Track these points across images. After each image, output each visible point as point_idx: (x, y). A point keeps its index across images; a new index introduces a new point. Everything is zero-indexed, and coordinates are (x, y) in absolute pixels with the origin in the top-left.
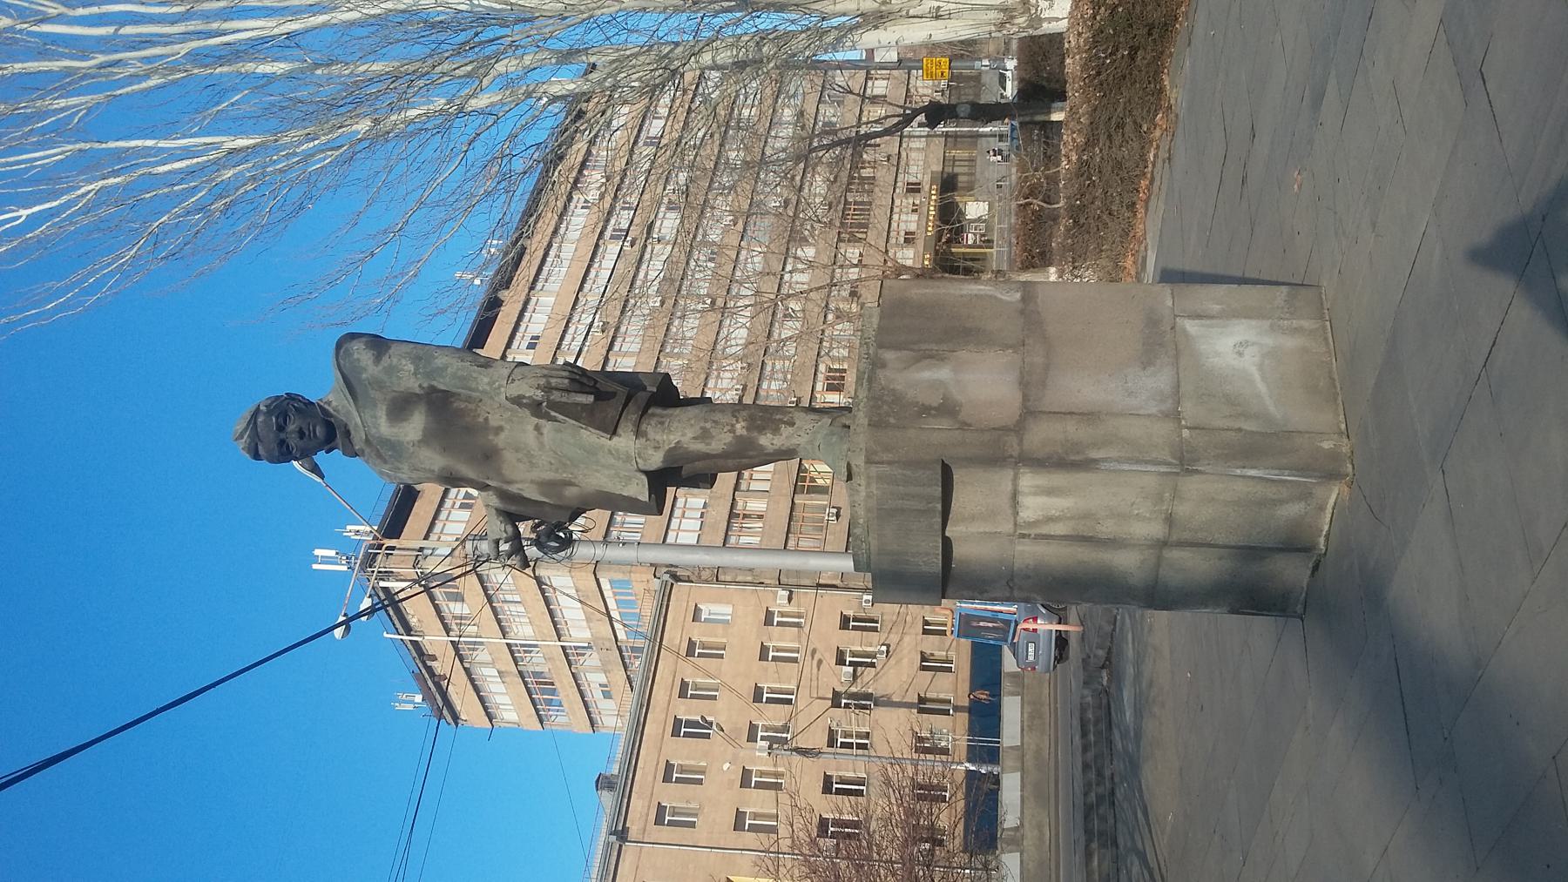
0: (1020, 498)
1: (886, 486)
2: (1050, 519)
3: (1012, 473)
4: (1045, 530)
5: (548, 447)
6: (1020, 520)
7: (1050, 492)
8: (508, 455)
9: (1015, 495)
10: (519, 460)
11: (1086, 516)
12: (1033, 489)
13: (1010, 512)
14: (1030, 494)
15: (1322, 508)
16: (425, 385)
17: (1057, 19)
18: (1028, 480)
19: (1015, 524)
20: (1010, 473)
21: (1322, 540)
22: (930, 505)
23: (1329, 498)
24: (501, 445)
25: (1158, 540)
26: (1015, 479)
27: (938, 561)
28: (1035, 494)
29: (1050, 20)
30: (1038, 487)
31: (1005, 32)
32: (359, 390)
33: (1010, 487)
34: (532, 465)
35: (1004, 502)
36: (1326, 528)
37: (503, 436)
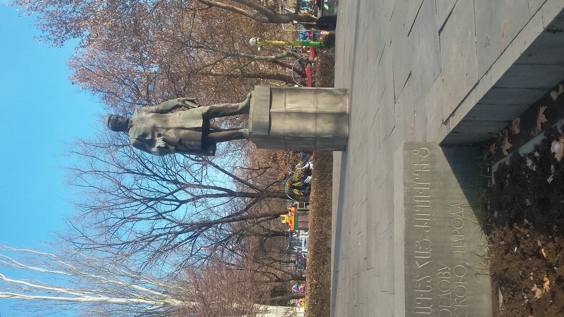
1: (258, 92)
2: (293, 108)
3: (284, 96)
4: (291, 110)
5: (181, 118)
6: (286, 109)
7: (292, 102)
8: (171, 121)
9: (285, 103)
10: (173, 122)
11: (300, 108)
12: (289, 102)
13: (284, 107)
14: (288, 103)
15: (346, 105)
16: (157, 108)
18: (288, 99)
19: (285, 109)
21: (348, 111)
22: (267, 98)
23: (347, 101)
24: (170, 119)
25: (315, 111)
26: (285, 98)
27: (268, 120)
28: (289, 103)
29: (299, 313)
30: (290, 101)
32: (139, 112)
33: (284, 101)
34: (176, 122)
36: (348, 109)
37: (171, 117)
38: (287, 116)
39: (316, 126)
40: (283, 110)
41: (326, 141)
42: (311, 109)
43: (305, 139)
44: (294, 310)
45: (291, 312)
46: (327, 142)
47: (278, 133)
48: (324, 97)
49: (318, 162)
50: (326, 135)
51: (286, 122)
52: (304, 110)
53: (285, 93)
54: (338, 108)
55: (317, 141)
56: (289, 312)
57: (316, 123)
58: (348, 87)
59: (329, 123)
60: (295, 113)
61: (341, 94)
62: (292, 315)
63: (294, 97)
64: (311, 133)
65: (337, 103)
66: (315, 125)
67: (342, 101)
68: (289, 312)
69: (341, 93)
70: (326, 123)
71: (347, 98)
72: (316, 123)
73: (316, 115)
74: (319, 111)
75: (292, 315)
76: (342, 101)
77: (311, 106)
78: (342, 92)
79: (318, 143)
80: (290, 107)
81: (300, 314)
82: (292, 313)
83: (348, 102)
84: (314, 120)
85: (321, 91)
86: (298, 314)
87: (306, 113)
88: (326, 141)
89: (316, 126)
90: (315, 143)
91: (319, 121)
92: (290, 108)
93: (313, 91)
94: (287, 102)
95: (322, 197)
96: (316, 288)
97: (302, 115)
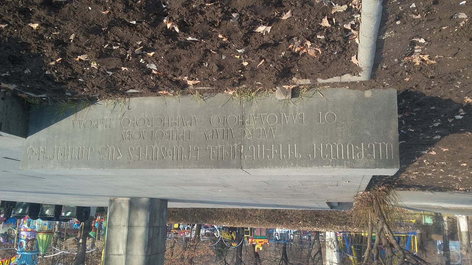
0: (119, 254)
2: (123, 248)
7: (118, 248)
12: (118, 251)
13: (122, 256)
14: (119, 252)
15: (123, 200)
17: (330, 234)
18: (115, 252)
19: (123, 255)
20: (112, 256)
21: (128, 199)
23: (120, 199)
26: (115, 255)
28: (119, 251)
29: (330, 236)
30: (117, 251)
31: (333, 248)
33: (117, 256)
35: (120, 257)
38: (130, 253)
39: (140, 226)
40: (123, 257)
41: (154, 218)
42: (125, 231)
43: (151, 237)
44: (328, 240)
45: (330, 243)
46: (155, 217)
47: (144, 262)
48: (115, 219)
49: (200, 219)
50: (148, 218)
51: (135, 254)
52: (125, 237)
53: (110, 255)
54: (126, 207)
55: (154, 226)
56: (330, 245)
57: (137, 226)
58: (108, 199)
59: (137, 215)
60: (128, 246)
61: (114, 204)
62: (333, 242)
63: (114, 246)
64: (146, 231)
65: (121, 208)
66: (139, 227)
67: (120, 203)
68: (330, 245)
69: (113, 205)
70: (138, 218)
71: (118, 199)
72: (137, 226)
73: (130, 227)
74: (127, 224)
75: (333, 242)
76: (120, 203)
77: (122, 231)
78: (112, 204)
79: (156, 224)
80: (122, 250)
81: (331, 235)
82: (331, 243)
83: (121, 199)
84: (135, 228)
85: (110, 223)
86: (331, 237)
87: (128, 236)
88: (154, 218)
89: (140, 226)
90: (157, 227)
91: (136, 224)
92: (122, 250)
93: (110, 230)
94: (118, 253)
95: (230, 216)
96: (306, 221)
97: (129, 240)
